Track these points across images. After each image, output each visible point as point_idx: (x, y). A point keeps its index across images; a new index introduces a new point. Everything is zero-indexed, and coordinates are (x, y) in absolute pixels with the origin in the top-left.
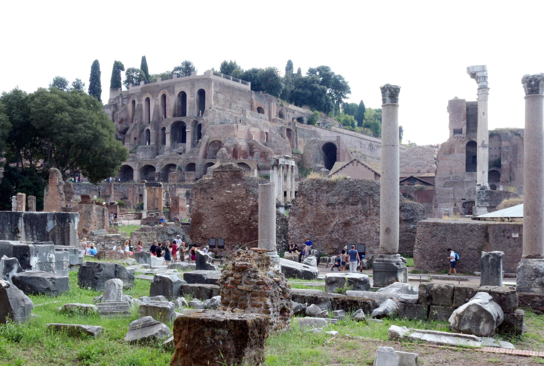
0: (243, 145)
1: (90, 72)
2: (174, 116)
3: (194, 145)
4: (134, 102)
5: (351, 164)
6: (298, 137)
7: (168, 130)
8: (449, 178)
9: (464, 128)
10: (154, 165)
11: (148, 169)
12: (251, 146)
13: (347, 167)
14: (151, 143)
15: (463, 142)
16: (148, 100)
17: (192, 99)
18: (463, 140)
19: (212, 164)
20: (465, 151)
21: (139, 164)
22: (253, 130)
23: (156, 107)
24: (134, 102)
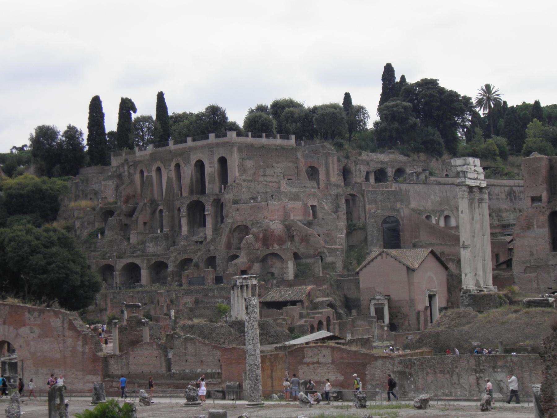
0: (277, 227)
1: (87, 115)
2: (191, 192)
3: (216, 230)
4: (142, 172)
5: (379, 258)
6: (367, 203)
7: (184, 211)
8: (530, 260)
9: (545, 196)
10: (166, 261)
11: (159, 268)
12: (288, 228)
13: (376, 260)
14: (164, 230)
15: (543, 213)
16: (159, 170)
17: (212, 168)
18: (544, 210)
19: (236, 257)
20: (547, 224)
21: (148, 260)
22: (291, 205)
23: (169, 179)
24: (142, 172)
